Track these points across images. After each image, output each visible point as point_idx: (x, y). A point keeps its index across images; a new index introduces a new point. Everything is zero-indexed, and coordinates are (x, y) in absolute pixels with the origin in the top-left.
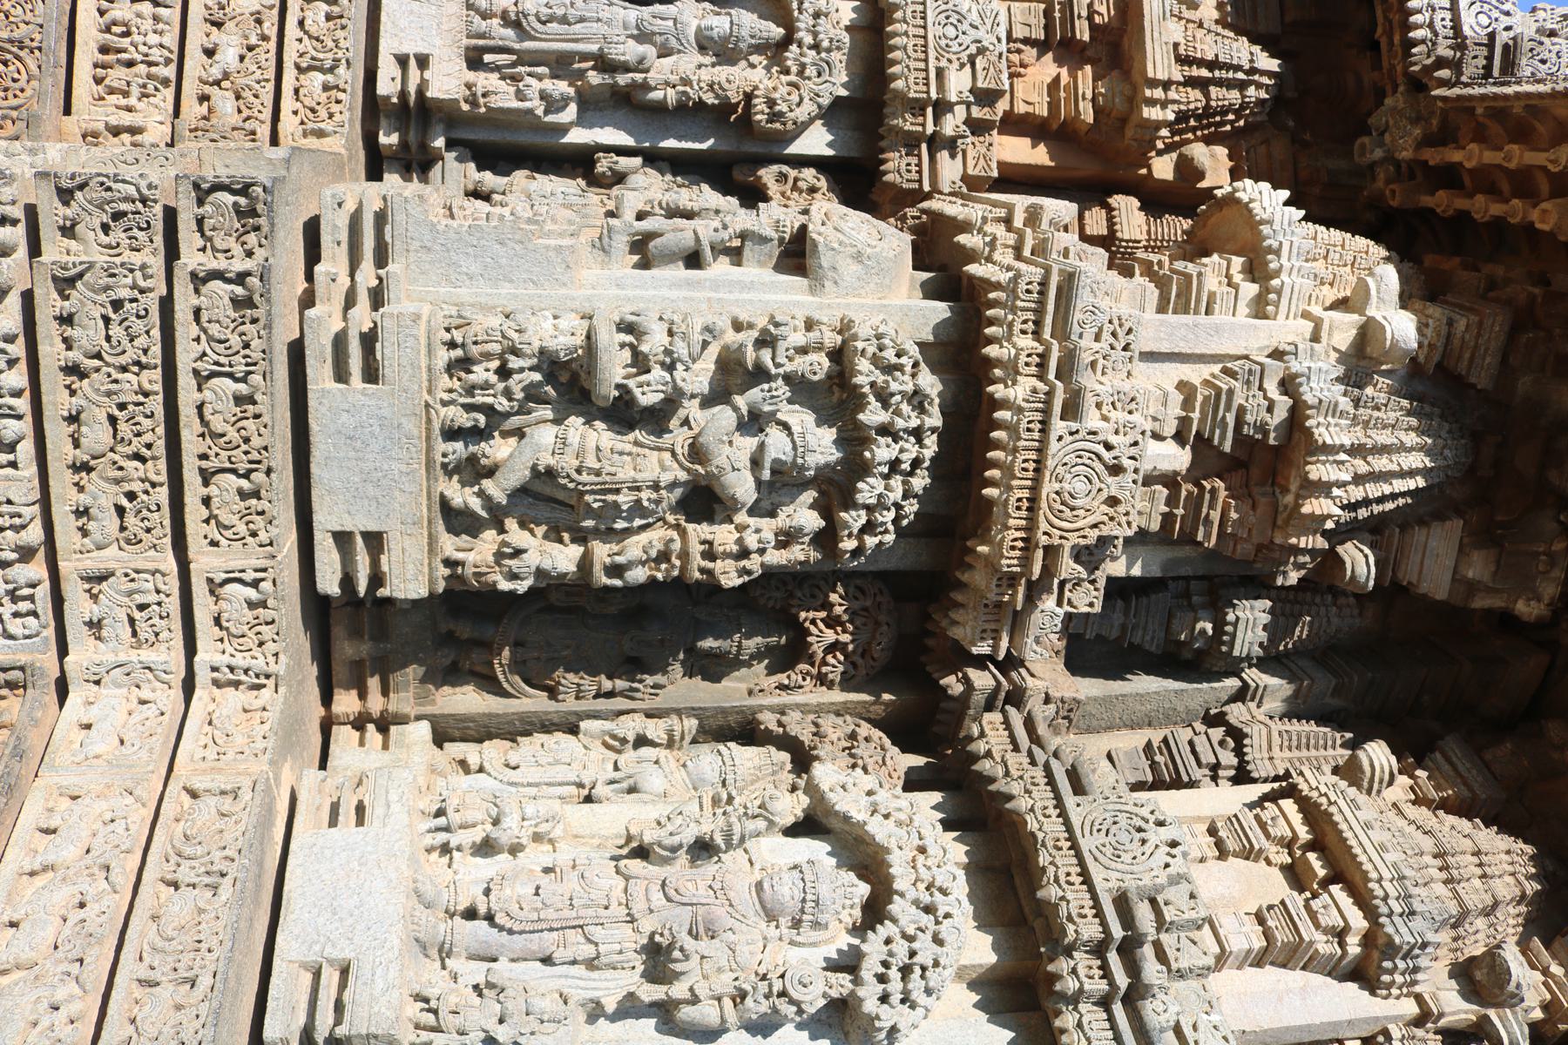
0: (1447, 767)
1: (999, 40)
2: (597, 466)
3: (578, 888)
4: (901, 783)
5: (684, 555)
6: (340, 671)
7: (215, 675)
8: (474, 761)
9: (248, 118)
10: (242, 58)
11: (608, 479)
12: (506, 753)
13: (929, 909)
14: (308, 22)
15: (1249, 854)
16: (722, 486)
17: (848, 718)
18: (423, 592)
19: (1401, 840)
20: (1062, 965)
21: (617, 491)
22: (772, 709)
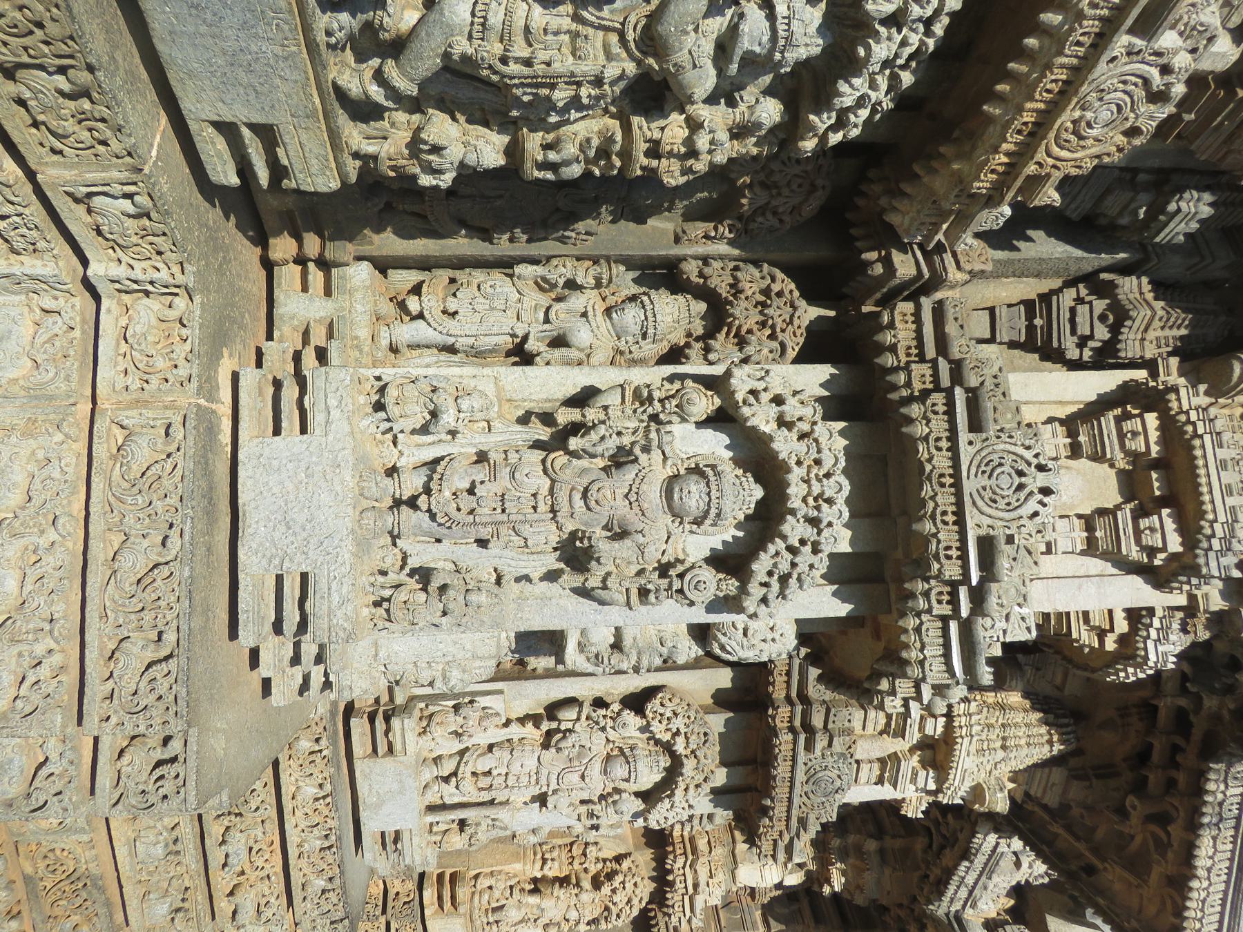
2: (525, 53)
3: (510, 486)
4: (801, 340)
5: (626, 154)
6: (269, 222)
7: (117, 286)
8: (413, 304)
11: (539, 68)
12: (444, 300)
13: (814, 522)
15: (1098, 457)
16: (681, 86)
17: (766, 265)
18: (335, 185)
20: (920, 586)
21: (553, 87)
22: (696, 258)
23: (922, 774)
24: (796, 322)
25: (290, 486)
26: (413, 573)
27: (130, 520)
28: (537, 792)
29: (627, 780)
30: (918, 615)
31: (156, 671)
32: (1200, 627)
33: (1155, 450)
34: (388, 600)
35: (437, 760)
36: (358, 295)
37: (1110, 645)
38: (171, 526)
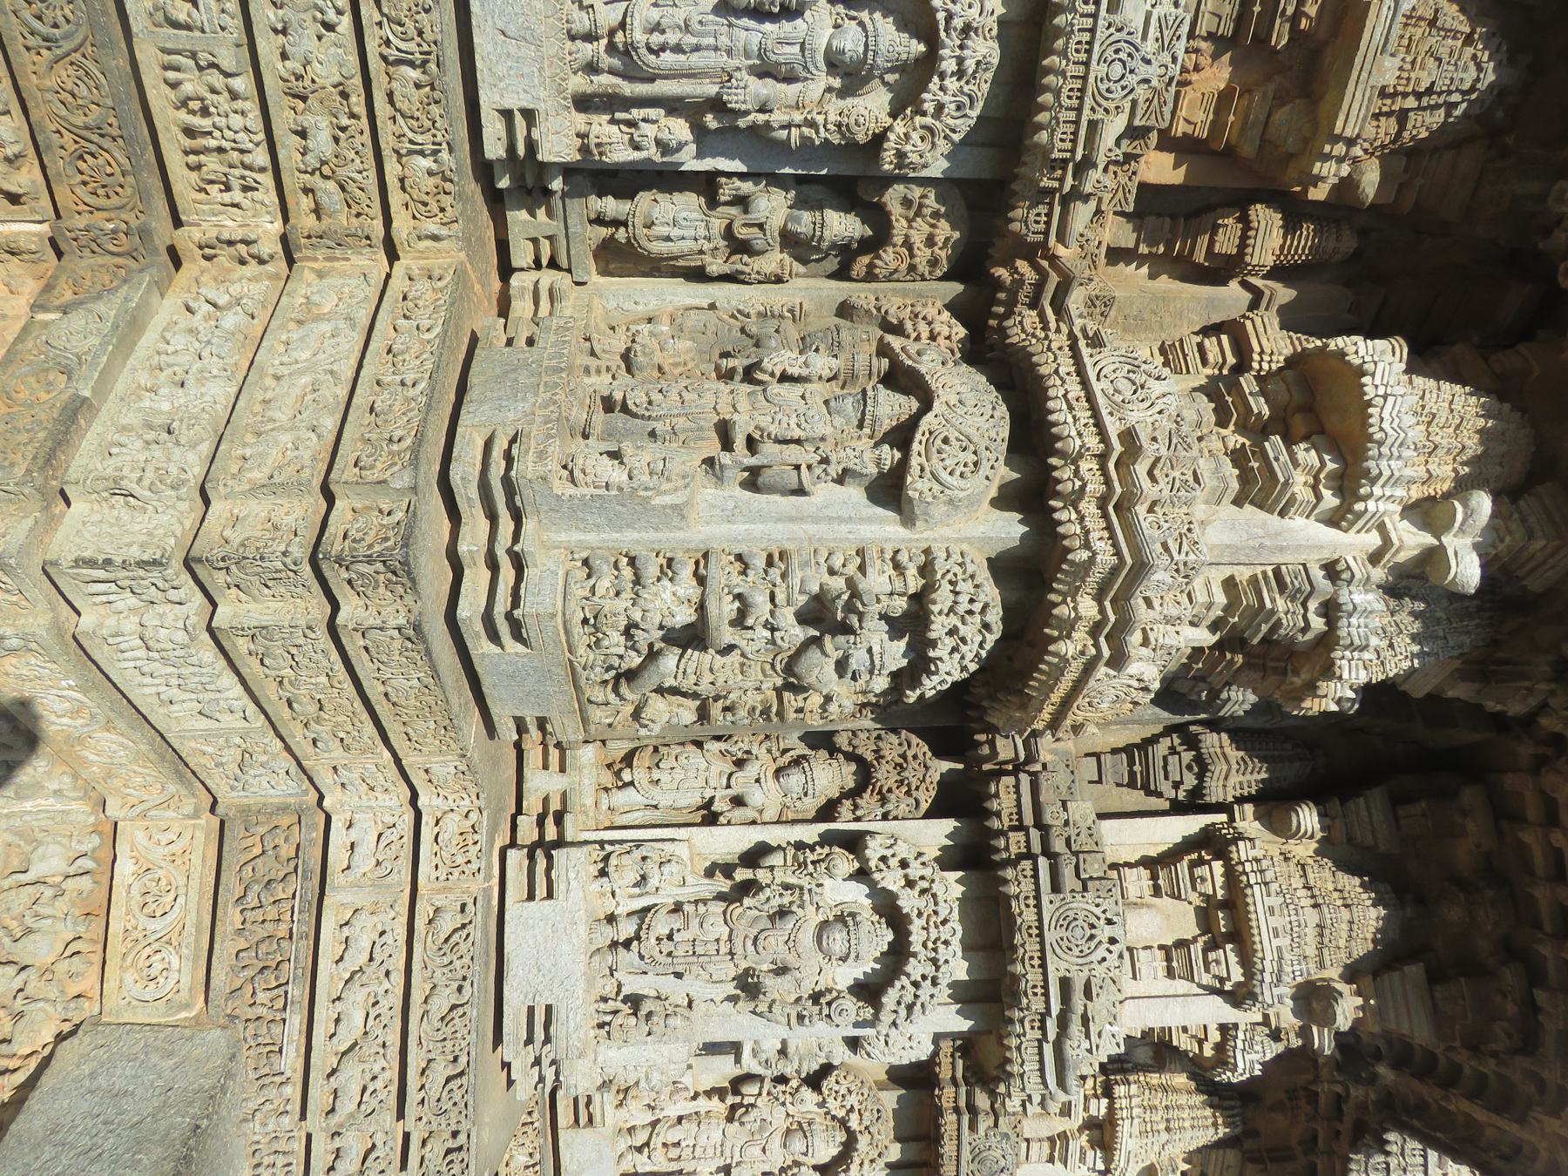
0: (1364, 813)
1: (1174, 60)
4: (933, 794)
8: (626, 776)
9: (358, 215)
10: (336, 140)
13: (934, 961)
14: (397, 97)
19: (1293, 918)
20: (1017, 1014)
23: (1090, 1154)
24: (928, 780)
25: (541, 940)
26: (626, 1000)
27: (438, 973)
28: (722, 1164)
29: (806, 1154)
30: (1019, 1036)
31: (454, 1085)
32: (1292, 1035)
33: (1220, 893)
34: (609, 1024)
35: (631, 1130)
36: (586, 771)
37: (1208, 1052)
38: (464, 978)
